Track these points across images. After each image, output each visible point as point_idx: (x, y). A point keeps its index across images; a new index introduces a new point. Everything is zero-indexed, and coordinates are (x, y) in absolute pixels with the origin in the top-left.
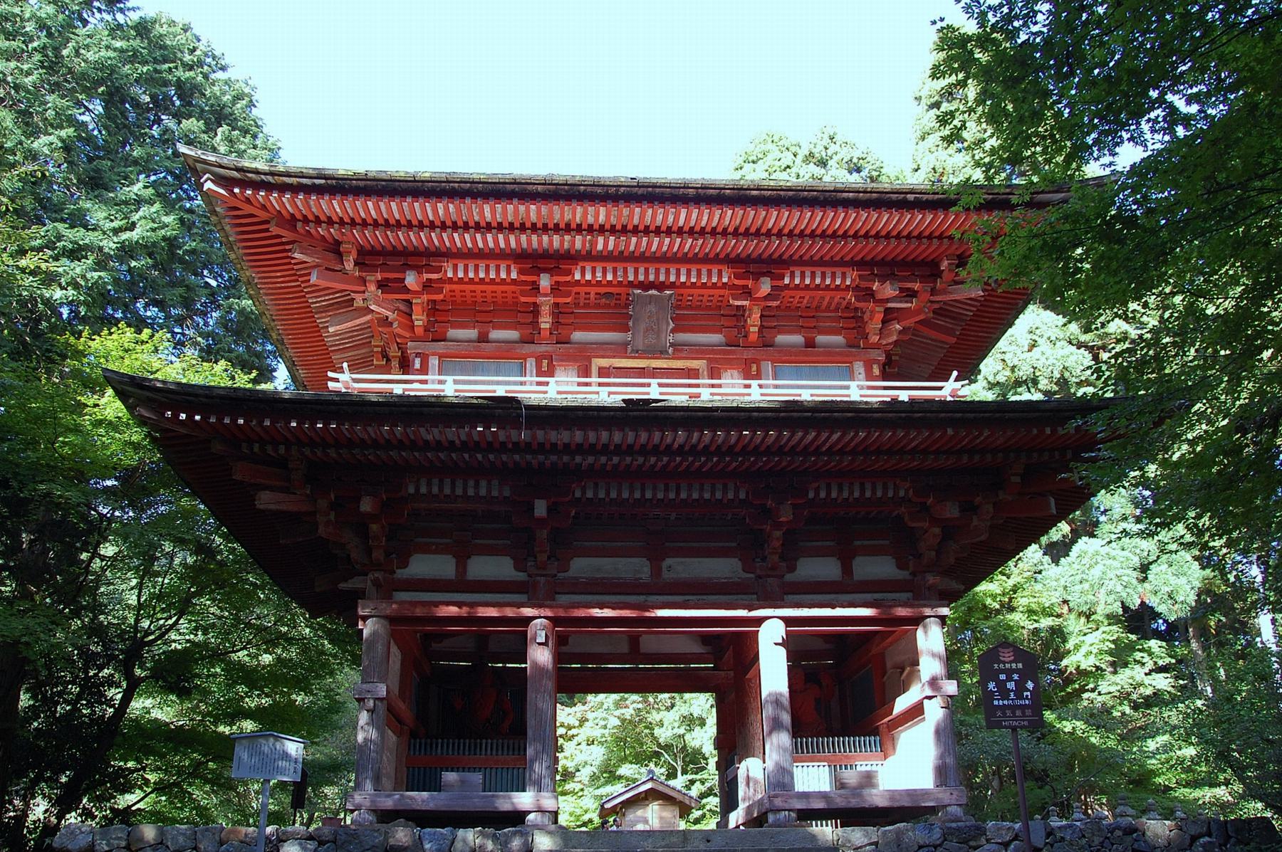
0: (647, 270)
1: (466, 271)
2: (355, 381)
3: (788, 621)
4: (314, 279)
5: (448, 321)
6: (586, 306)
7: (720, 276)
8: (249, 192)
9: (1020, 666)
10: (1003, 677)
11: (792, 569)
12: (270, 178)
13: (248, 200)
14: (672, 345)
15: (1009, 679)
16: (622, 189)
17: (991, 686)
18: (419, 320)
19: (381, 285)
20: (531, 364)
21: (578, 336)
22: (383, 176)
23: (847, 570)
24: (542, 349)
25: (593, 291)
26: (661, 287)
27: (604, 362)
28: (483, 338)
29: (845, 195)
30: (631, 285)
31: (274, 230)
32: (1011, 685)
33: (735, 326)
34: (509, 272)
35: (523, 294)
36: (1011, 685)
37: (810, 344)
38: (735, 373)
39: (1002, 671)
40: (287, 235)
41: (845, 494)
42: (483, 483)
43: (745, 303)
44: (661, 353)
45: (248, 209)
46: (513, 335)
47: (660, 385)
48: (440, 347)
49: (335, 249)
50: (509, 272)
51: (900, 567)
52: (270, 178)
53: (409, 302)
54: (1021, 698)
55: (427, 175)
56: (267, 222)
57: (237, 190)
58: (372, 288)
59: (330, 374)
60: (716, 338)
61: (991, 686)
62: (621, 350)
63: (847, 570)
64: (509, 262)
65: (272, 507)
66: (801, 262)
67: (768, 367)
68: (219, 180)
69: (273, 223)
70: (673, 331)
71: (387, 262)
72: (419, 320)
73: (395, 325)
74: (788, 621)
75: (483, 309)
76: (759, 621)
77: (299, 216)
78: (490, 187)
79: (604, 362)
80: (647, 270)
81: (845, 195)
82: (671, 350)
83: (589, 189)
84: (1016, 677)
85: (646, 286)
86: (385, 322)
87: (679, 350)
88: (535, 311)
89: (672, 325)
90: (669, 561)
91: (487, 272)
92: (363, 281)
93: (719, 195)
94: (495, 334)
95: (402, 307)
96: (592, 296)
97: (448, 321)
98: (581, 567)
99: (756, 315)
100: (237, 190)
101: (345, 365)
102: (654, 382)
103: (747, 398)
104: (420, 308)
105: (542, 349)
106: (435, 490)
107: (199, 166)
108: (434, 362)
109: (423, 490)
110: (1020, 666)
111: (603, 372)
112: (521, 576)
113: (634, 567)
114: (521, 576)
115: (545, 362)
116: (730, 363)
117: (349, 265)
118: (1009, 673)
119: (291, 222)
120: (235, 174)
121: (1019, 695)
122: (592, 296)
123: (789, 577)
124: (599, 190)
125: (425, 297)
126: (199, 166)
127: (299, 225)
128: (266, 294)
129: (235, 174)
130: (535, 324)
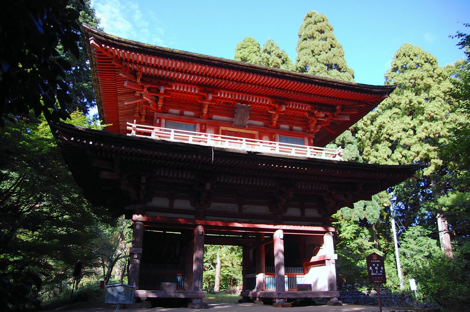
0: (242, 96)
1: (180, 88)
2: (137, 127)
3: (284, 231)
4: (126, 84)
5: (169, 106)
6: (218, 106)
7: (266, 102)
8: (108, 47)
9: (379, 261)
10: (374, 265)
11: (286, 211)
12: (117, 43)
13: (106, 50)
14: (248, 124)
15: (376, 266)
16: (244, 67)
17: (371, 268)
18: (160, 104)
19: (149, 89)
20: (198, 126)
21: (215, 117)
22: (161, 49)
23: (303, 212)
24: (203, 121)
25: (222, 101)
26: (247, 103)
27: (224, 128)
28: (181, 114)
29: (316, 80)
30: (237, 101)
31: (113, 63)
32: (376, 268)
33: (267, 120)
34: (195, 91)
35: (199, 99)
36: (376, 268)
37: (291, 129)
38: (267, 137)
39: (374, 263)
40: (118, 65)
41: (306, 187)
42: (185, 173)
43: (273, 112)
44: (243, 127)
45: (105, 53)
46: (192, 114)
47: (247, 141)
48: (166, 115)
49: (134, 73)
50: (195, 91)
51: (320, 213)
52: (117, 43)
53: (157, 97)
54: (379, 272)
55: (178, 51)
56: (111, 59)
57: (103, 45)
58: (145, 90)
59: (128, 123)
60: (260, 123)
61: (371, 268)
62: (230, 124)
63: (303, 212)
64: (195, 87)
65: (106, 178)
66: (293, 100)
67: (278, 136)
68: (96, 40)
69: (114, 60)
70: (249, 119)
71: (153, 82)
72: (160, 104)
73: (151, 105)
74: (284, 231)
75: (182, 103)
76: (275, 230)
77: (124, 59)
78: (198, 59)
79: (224, 128)
80: (242, 96)
81: (316, 80)
82: (247, 127)
83: (233, 65)
84: (378, 265)
85: (242, 102)
86: (146, 103)
87: (251, 127)
88: (201, 106)
89: (249, 117)
90: (245, 206)
91: (187, 89)
92: (143, 88)
93: (269, 73)
94: (186, 113)
95: (154, 98)
96: (221, 103)
97: (169, 106)
98: (215, 206)
99: (277, 117)
100: (103, 45)
101: (135, 121)
102: (244, 139)
103: (289, 154)
104: (162, 100)
105: (203, 121)
106: (167, 174)
107: (89, 33)
108: (163, 121)
109: (162, 174)
110: (379, 261)
111: (224, 133)
112: (193, 208)
113: (232, 207)
114: (193, 208)
115: (204, 126)
116: (266, 134)
117: (138, 81)
118: (376, 263)
119: (120, 60)
120: (104, 39)
121: (379, 272)
122: (221, 103)
123: (285, 214)
124: (236, 66)
125: (164, 96)
126: (89, 33)
127: (123, 62)
128: (101, 86)
129: (104, 39)
130: (201, 111)
